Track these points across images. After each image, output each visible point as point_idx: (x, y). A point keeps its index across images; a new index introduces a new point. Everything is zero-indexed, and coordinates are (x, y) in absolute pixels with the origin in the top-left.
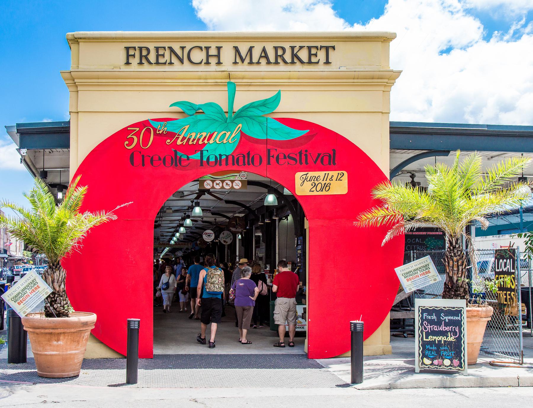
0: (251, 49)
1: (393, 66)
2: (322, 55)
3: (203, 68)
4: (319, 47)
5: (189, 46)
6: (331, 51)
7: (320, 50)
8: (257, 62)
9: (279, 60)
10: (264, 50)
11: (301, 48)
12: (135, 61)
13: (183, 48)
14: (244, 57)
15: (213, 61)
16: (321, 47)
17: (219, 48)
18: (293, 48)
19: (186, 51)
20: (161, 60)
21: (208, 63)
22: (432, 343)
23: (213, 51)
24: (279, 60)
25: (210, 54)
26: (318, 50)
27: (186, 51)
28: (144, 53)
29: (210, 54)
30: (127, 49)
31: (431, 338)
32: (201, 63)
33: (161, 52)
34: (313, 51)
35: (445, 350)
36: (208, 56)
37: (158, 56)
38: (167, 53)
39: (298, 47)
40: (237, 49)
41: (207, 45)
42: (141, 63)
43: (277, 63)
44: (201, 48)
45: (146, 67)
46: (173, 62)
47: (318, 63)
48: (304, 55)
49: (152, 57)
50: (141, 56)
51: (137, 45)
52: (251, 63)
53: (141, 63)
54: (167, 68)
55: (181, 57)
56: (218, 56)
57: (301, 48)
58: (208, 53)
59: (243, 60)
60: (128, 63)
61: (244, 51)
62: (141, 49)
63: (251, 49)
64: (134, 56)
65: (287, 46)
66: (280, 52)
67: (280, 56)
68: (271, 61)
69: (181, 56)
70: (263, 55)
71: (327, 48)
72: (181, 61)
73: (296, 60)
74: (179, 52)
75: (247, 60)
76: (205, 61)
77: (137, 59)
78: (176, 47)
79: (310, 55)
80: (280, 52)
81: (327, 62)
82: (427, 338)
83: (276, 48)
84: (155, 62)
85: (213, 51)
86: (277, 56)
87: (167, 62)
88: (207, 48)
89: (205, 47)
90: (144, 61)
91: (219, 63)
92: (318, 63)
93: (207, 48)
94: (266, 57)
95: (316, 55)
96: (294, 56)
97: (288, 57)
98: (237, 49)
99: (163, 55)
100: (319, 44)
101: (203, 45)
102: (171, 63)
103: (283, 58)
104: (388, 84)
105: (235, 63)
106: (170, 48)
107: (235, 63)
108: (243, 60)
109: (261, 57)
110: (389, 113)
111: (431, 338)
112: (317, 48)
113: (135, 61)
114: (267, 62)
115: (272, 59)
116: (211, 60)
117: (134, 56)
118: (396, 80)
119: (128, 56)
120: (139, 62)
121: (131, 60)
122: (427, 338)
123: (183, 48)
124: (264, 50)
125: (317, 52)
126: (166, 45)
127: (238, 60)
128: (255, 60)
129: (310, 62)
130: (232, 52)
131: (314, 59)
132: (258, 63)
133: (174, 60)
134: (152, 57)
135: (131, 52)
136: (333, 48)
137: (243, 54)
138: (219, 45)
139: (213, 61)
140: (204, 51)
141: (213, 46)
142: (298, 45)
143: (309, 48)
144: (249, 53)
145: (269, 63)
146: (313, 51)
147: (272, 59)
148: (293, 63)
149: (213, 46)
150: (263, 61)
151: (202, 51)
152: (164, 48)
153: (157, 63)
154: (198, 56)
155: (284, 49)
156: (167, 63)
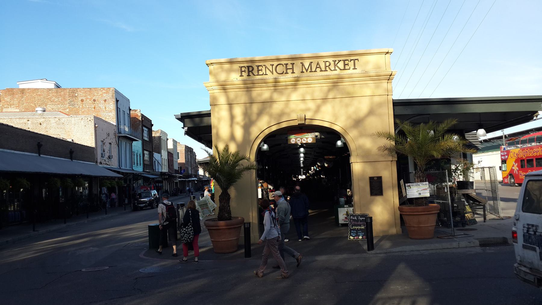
7: (350, 62)
9: (327, 68)
11: (340, 61)
19: (274, 67)
21: (286, 73)
22: (354, 230)
23: (290, 66)
24: (327, 68)
27: (274, 67)
28: (251, 69)
31: (354, 227)
34: (346, 62)
35: (360, 232)
37: (258, 70)
38: (264, 69)
50: (249, 72)
56: (293, 69)
58: (286, 67)
69: (271, 70)
73: (337, 68)
75: (309, 70)
79: (345, 65)
82: (352, 227)
86: (326, 67)
99: (261, 70)
109: (317, 68)
111: (354, 227)
115: (323, 69)
122: (352, 227)
127: (304, 70)
128: (313, 70)
132: (315, 71)
133: (268, 72)
139: (290, 71)
143: (344, 61)
145: (321, 71)
147: (323, 69)
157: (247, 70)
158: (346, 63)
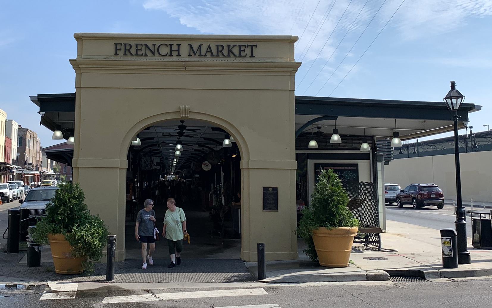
0: (200, 46)
1: (297, 60)
2: (248, 51)
3: (167, 59)
4: (246, 45)
5: (158, 43)
6: (254, 48)
7: (247, 47)
8: (204, 55)
10: (209, 47)
11: (234, 46)
12: (121, 53)
13: (154, 45)
14: (196, 52)
15: (175, 53)
16: (248, 46)
17: (179, 46)
18: (229, 46)
19: (156, 47)
20: (140, 53)
21: (171, 55)
23: (175, 48)
24: (220, 54)
25: (172, 49)
26: (246, 47)
27: (156, 47)
28: (128, 48)
29: (172, 49)
30: (116, 45)
32: (166, 55)
33: (139, 47)
36: (171, 51)
38: (143, 48)
39: (232, 45)
40: (191, 46)
41: (171, 43)
42: (125, 54)
43: (218, 56)
44: (166, 45)
45: (129, 58)
46: (147, 54)
47: (246, 56)
48: (236, 51)
49: (133, 51)
50: (125, 50)
51: (123, 42)
52: (200, 55)
53: (125, 54)
54: (143, 59)
55: (153, 51)
57: (234, 46)
59: (195, 54)
60: (116, 54)
61: (195, 48)
62: (125, 45)
63: (200, 46)
64: (121, 49)
65: (225, 44)
66: (220, 49)
67: (220, 51)
68: (214, 55)
69: (153, 50)
70: (209, 50)
71: (252, 47)
72: (153, 53)
73: (231, 54)
74: (151, 47)
75: (198, 54)
76: (169, 53)
77: (123, 52)
78: (150, 44)
79: (240, 51)
80: (220, 49)
81: (252, 56)
83: (217, 46)
84: (135, 54)
85: (175, 48)
86: (218, 51)
87: (144, 54)
88: (171, 45)
89: (169, 44)
90: (127, 53)
91: (179, 55)
92: (246, 56)
93: (171, 45)
94: (211, 51)
95: (244, 51)
96: (230, 51)
97: (225, 52)
98: (191, 46)
99: (141, 49)
100: (246, 44)
101: (168, 43)
102: (146, 55)
103: (222, 52)
104: (293, 71)
105: (190, 55)
106: (146, 45)
107: (190, 55)
108: (195, 54)
109: (207, 51)
110: (294, 90)
112: (245, 46)
113: (121, 53)
114: (211, 55)
115: (215, 53)
116: (173, 53)
117: (121, 49)
118: (298, 69)
119: (116, 50)
120: (124, 54)
121: (118, 52)
123: (154, 45)
124: (209, 47)
125: (245, 49)
126: (143, 43)
127: (192, 53)
128: (203, 53)
129: (240, 56)
130: (188, 48)
131: (243, 54)
132: (205, 56)
133: (148, 53)
134: (133, 51)
135: (119, 47)
136: (256, 46)
137: (195, 49)
138: (179, 43)
139: (175, 53)
140: (169, 48)
141: (175, 43)
142: (232, 44)
143: (240, 46)
144: (199, 49)
145: (212, 55)
146: (243, 48)
147: (215, 53)
148: (229, 56)
149: (175, 43)
150: (209, 54)
151: (167, 47)
152: (142, 44)
153: (137, 54)
154: (164, 50)
155: (223, 47)
156: (143, 55)
157: (123, 48)
158: (242, 49)
